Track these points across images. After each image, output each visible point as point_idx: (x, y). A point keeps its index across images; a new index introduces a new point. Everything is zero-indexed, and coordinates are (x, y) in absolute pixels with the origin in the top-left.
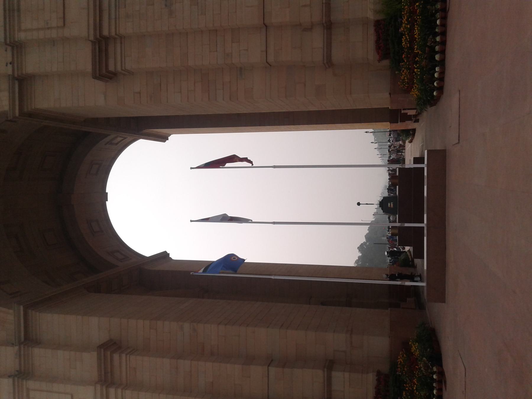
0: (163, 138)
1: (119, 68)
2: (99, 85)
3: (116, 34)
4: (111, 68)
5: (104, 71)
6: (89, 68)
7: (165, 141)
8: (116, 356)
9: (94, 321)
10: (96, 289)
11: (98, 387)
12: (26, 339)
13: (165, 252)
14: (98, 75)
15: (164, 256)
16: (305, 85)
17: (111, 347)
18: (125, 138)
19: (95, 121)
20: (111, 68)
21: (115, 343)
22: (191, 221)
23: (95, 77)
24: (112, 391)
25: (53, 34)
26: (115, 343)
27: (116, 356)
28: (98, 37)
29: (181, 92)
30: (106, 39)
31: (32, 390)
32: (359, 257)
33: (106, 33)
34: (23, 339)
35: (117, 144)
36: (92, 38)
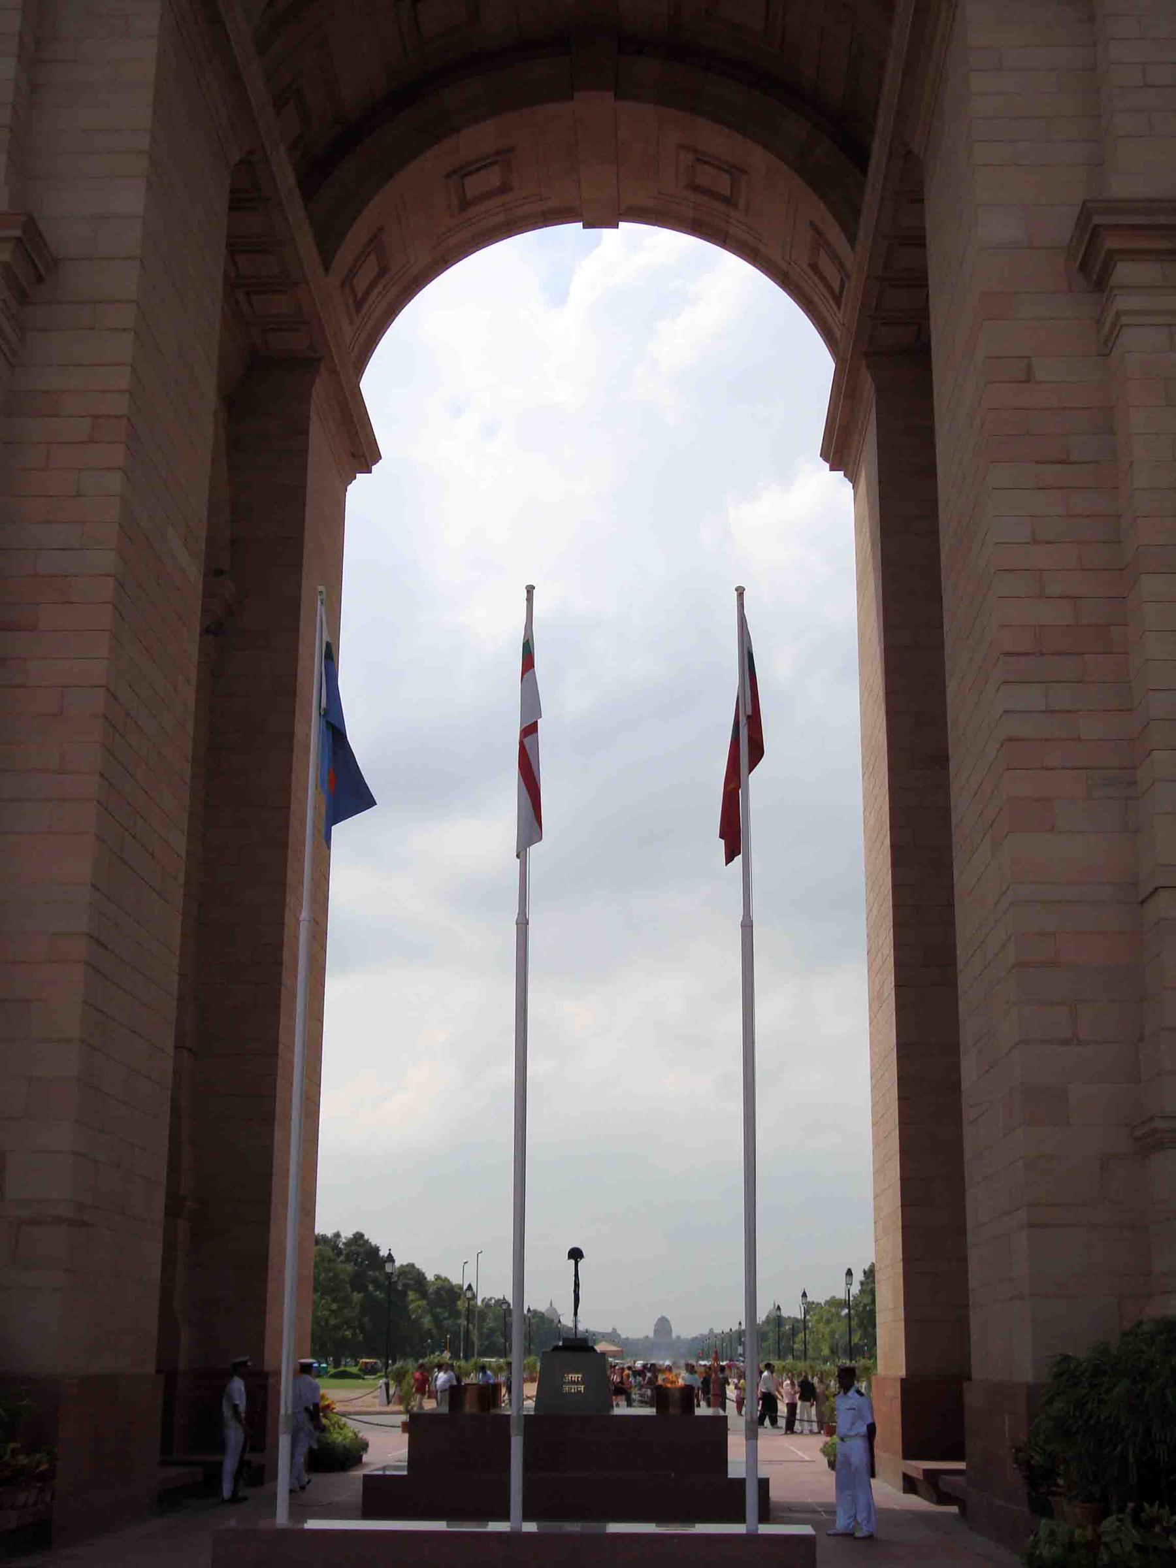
1: (1123, 302)
4: (1124, 271)
5: (1111, 243)
7: (825, 455)
9: (130, 199)
10: (246, 195)
13: (376, 456)
14: (1097, 220)
15: (364, 454)
16: (1065, 1042)
19: (910, 191)
21: (40, 279)
22: (530, 590)
23: (1085, 213)
26: (40, 279)
29: (1035, 542)
32: (619, 1336)
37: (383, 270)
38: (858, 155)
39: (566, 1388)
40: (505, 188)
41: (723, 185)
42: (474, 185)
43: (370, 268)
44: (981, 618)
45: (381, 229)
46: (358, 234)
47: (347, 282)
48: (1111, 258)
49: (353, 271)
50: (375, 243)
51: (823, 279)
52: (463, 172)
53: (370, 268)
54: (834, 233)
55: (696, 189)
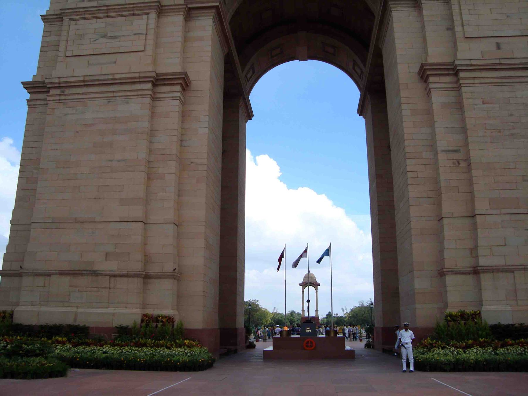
0: (361, 111)
2: (416, 69)
3: (460, 84)
4: (431, 79)
5: (428, 73)
6: (430, 60)
7: (358, 112)
8: (178, 88)
10: (228, 61)
11: (153, 74)
12: (190, 9)
13: (253, 116)
14: (425, 67)
17: (184, 82)
19: (378, 54)
20: (431, 79)
21: (188, 86)
23: (422, 66)
24: (149, 86)
25: (458, 29)
27: (178, 88)
28: (458, 68)
30: (456, 74)
31: (148, 17)
33: (462, 75)
34: (190, 6)
35: (355, 71)
36: (457, 63)
37: (254, 73)
38: (366, 46)
39: (307, 331)
45: (253, 64)
46: (248, 66)
47: (246, 76)
48: (428, 76)
49: (247, 74)
50: (252, 68)
51: (357, 73)
53: (251, 72)
54: (359, 62)
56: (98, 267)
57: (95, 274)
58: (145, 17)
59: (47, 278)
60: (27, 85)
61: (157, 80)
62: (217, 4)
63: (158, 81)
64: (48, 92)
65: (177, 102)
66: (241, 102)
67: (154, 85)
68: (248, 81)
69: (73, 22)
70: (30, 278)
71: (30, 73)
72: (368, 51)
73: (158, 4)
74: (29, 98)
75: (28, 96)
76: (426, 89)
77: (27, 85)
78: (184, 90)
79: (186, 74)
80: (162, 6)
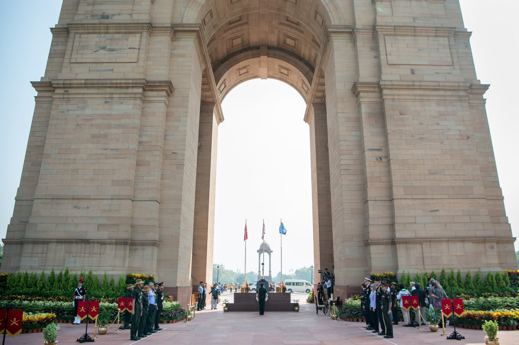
0: (306, 119)
2: (349, 86)
6: (361, 80)
7: (304, 120)
8: (164, 93)
11: (144, 81)
15: (221, 119)
18: (307, 93)
24: (140, 90)
28: (382, 87)
34: (175, 29)
37: (225, 86)
38: (313, 69)
40: (247, 72)
41: (286, 72)
42: (242, 72)
43: (223, 86)
44: (340, 160)
47: (219, 88)
52: (239, 69)
53: (223, 86)
55: (281, 73)
56: (89, 236)
57: (87, 242)
58: (138, 35)
59: (46, 246)
60: (35, 84)
61: (146, 86)
62: (198, 29)
63: (148, 86)
64: (54, 91)
65: (163, 105)
66: (215, 109)
67: (144, 90)
68: (221, 92)
69: (77, 36)
70: (31, 246)
71: (39, 75)
72: (314, 73)
73: (149, 25)
74: (36, 95)
75: (36, 94)
76: (357, 102)
77: (35, 84)
78: (169, 95)
79: (170, 83)
80: (153, 27)
